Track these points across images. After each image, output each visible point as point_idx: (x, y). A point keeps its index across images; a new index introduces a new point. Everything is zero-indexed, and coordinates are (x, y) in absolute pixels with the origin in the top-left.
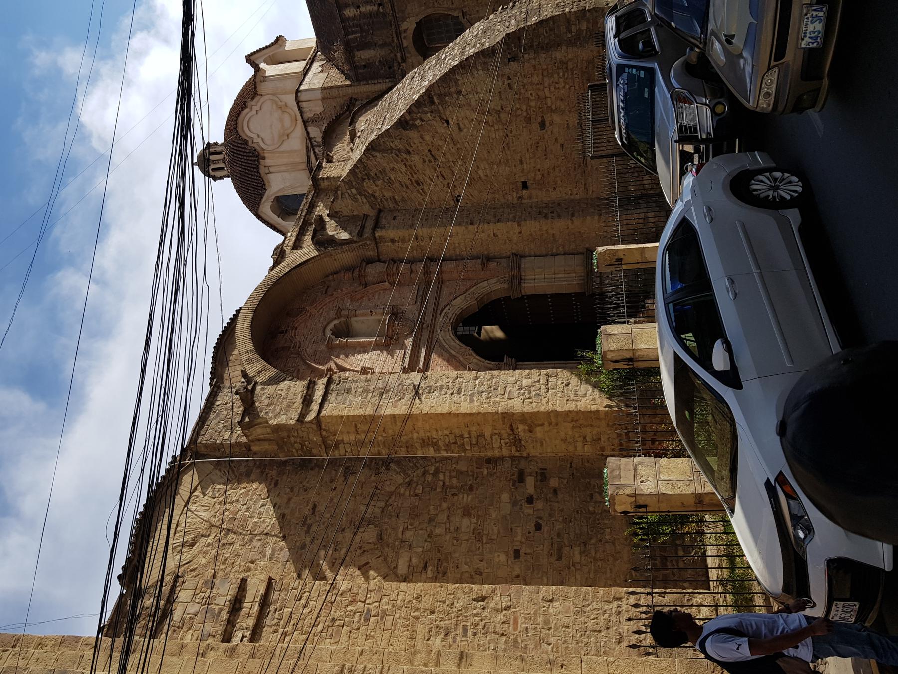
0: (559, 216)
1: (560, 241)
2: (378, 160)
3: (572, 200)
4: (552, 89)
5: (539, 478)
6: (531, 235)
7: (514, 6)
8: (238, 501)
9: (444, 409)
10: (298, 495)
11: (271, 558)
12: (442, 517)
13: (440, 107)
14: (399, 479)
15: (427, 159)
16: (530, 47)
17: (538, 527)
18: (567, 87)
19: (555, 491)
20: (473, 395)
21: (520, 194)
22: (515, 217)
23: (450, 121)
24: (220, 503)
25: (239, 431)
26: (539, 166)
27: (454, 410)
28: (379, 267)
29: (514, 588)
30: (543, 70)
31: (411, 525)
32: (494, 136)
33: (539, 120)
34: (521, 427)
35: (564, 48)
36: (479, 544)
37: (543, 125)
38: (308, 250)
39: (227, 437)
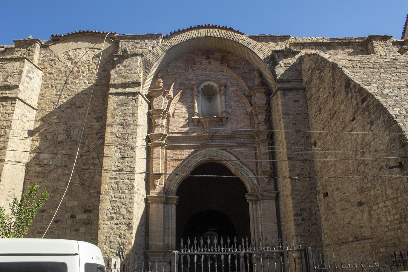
0: (297, 225)
1: (286, 227)
3: (319, 234)
4: (385, 209)
5: (86, 221)
8: (89, 71)
11: (56, 95)
13: (360, 110)
18: (388, 224)
20: (116, 178)
21: (321, 192)
22: (298, 190)
23: (354, 122)
24: (89, 63)
26: (336, 205)
30: (397, 198)
32: (350, 162)
33: (363, 200)
37: (360, 204)
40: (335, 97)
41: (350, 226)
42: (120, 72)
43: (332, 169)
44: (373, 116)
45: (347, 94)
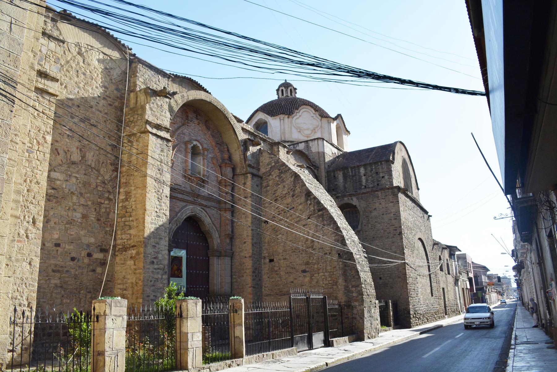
0: (253, 280)
2: (290, 179)
3: (261, 287)
4: (323, 277)
5: (102, 261)
6: (244, 263)
7: (365, 257)
9: (148, 206)
10: (103, 117)
12: (82, 201)
13: (316, 215)
14: (107, 177)
15: (289, 206)
16: (345, 265)
17: (73, 259)
19: (94, 271)
22: (254, 254)
25: (143, 87)
26: (282, 269)
27: (147, 212)
28: (230, 175)
29: (39, 242)
30: (333, 272)
31: (80, 182)
33: (307, 270)
34: (134, 252)
35: (344, 284)
36: (65, 222)
37: (304, 271)
38: (242, 136)
39: (140, 79)
40: (294, 197)
41: (292, 284)
42: (154, 109)
43: (282, 244)
44: (325, 222)
45: (307, 200)
